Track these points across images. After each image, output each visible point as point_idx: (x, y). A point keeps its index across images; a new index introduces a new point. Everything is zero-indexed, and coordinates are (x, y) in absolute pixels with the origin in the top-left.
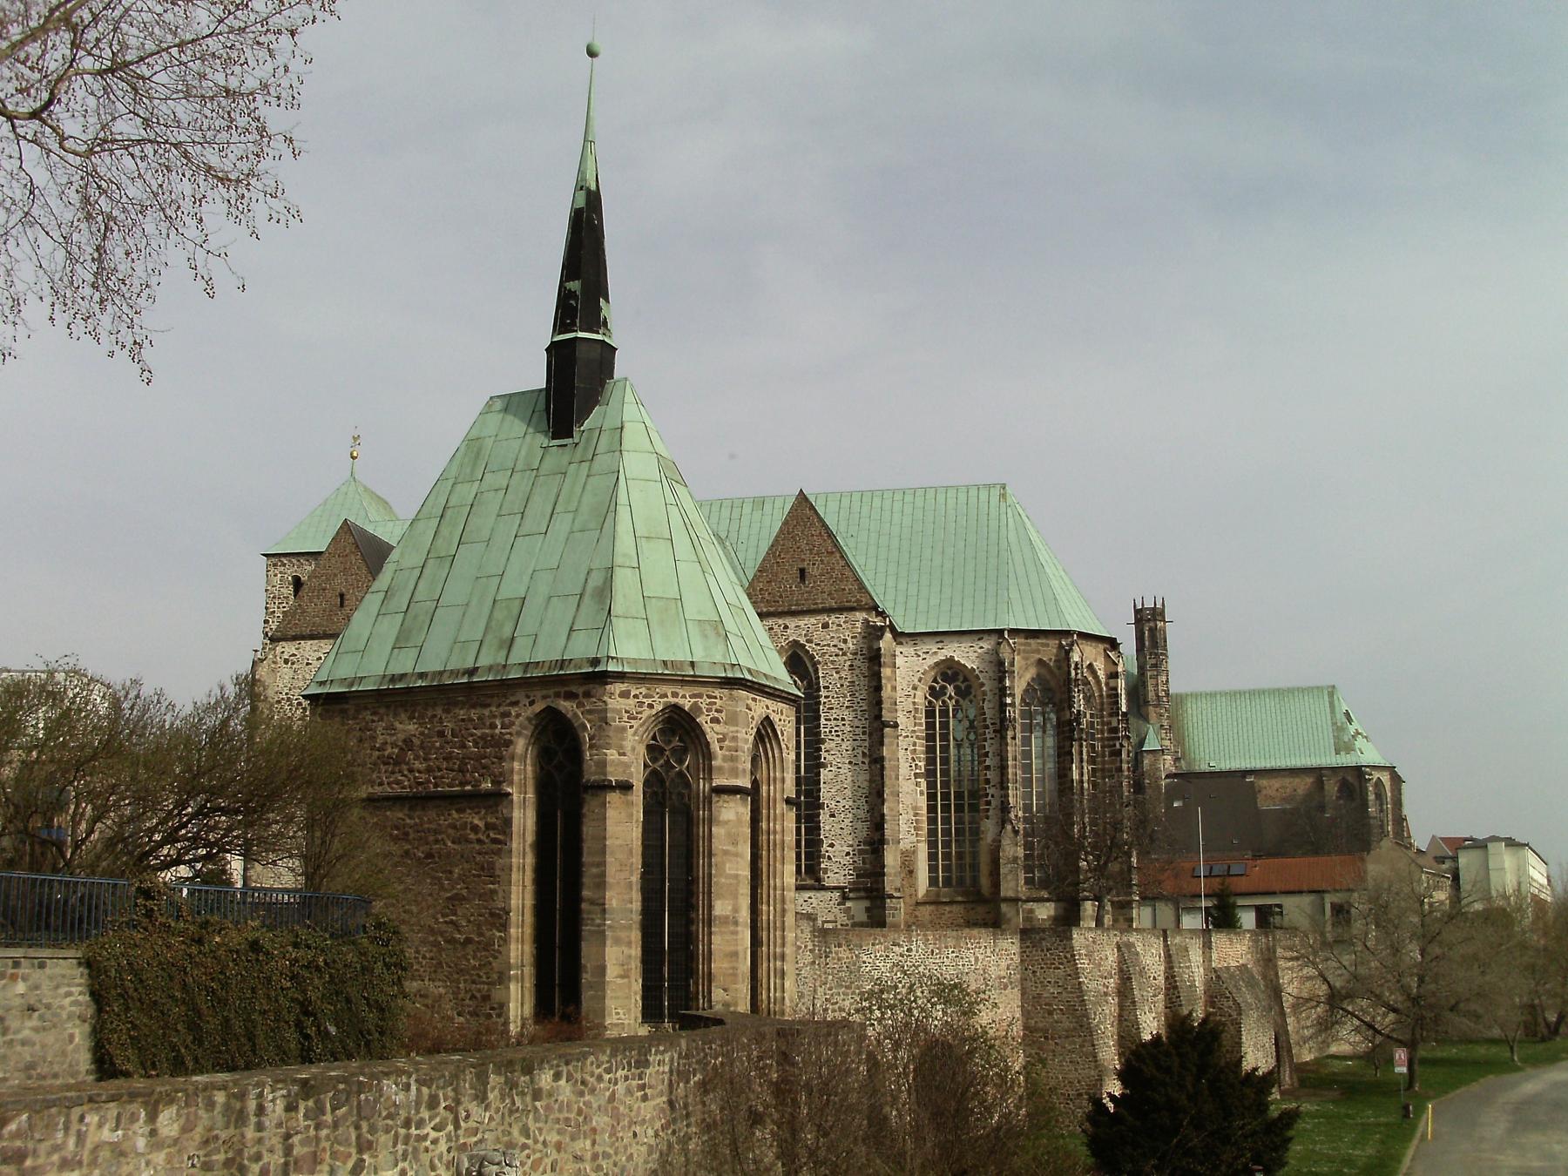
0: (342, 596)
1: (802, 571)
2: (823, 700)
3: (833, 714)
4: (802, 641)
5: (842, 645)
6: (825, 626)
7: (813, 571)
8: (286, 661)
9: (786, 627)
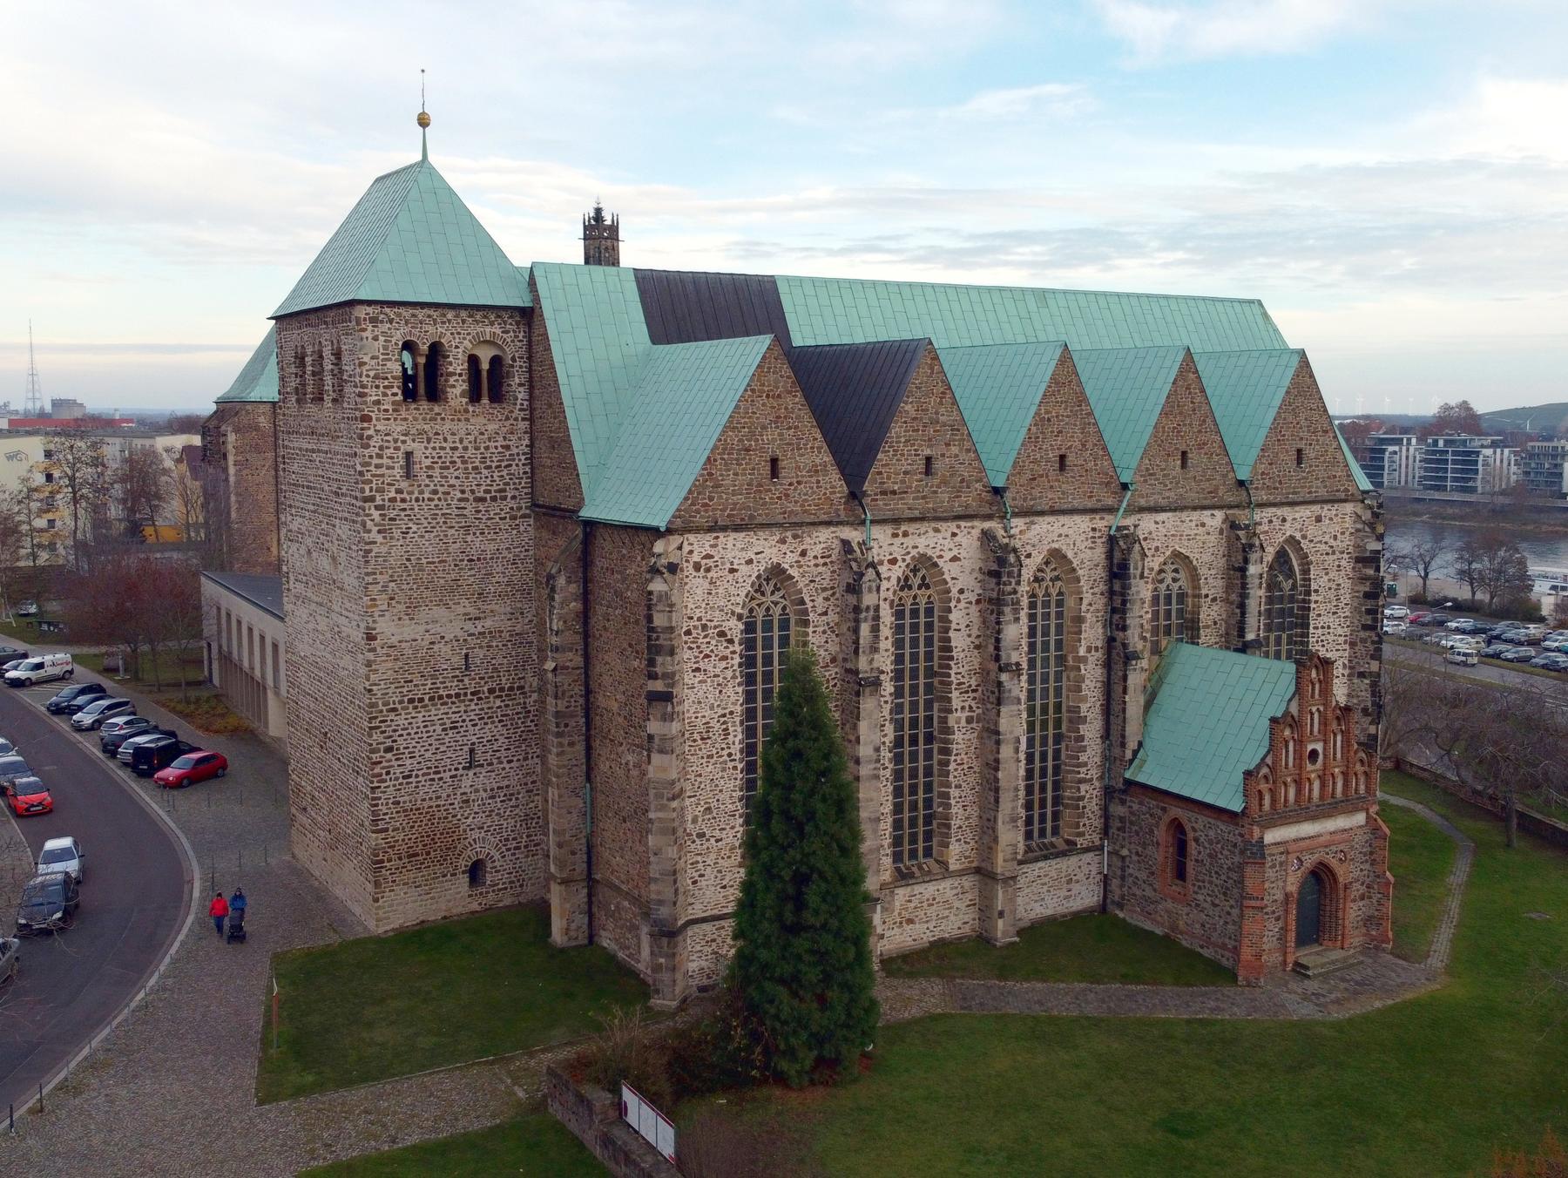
0: (774, 462)
1: (1299, 451)
2: (1313, 605)
3: (1320, 622)
4: (1298, 536)
6: (1319, 519)
7: (1310, 453)
8: (697, 567)
9: (1284, 520)
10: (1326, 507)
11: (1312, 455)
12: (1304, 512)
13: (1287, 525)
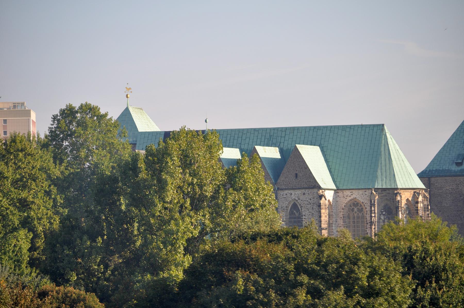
1: (296, 174)
4: (297, 199)
5: (309, 201)
9: (291, 194)
10: (307, 190)
11: (301, 175)
12: (298, 192)
13: (293, 195)
